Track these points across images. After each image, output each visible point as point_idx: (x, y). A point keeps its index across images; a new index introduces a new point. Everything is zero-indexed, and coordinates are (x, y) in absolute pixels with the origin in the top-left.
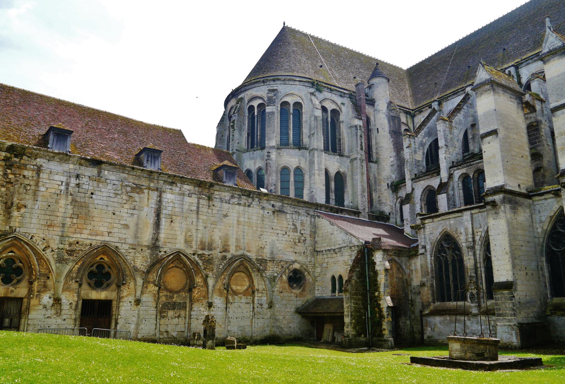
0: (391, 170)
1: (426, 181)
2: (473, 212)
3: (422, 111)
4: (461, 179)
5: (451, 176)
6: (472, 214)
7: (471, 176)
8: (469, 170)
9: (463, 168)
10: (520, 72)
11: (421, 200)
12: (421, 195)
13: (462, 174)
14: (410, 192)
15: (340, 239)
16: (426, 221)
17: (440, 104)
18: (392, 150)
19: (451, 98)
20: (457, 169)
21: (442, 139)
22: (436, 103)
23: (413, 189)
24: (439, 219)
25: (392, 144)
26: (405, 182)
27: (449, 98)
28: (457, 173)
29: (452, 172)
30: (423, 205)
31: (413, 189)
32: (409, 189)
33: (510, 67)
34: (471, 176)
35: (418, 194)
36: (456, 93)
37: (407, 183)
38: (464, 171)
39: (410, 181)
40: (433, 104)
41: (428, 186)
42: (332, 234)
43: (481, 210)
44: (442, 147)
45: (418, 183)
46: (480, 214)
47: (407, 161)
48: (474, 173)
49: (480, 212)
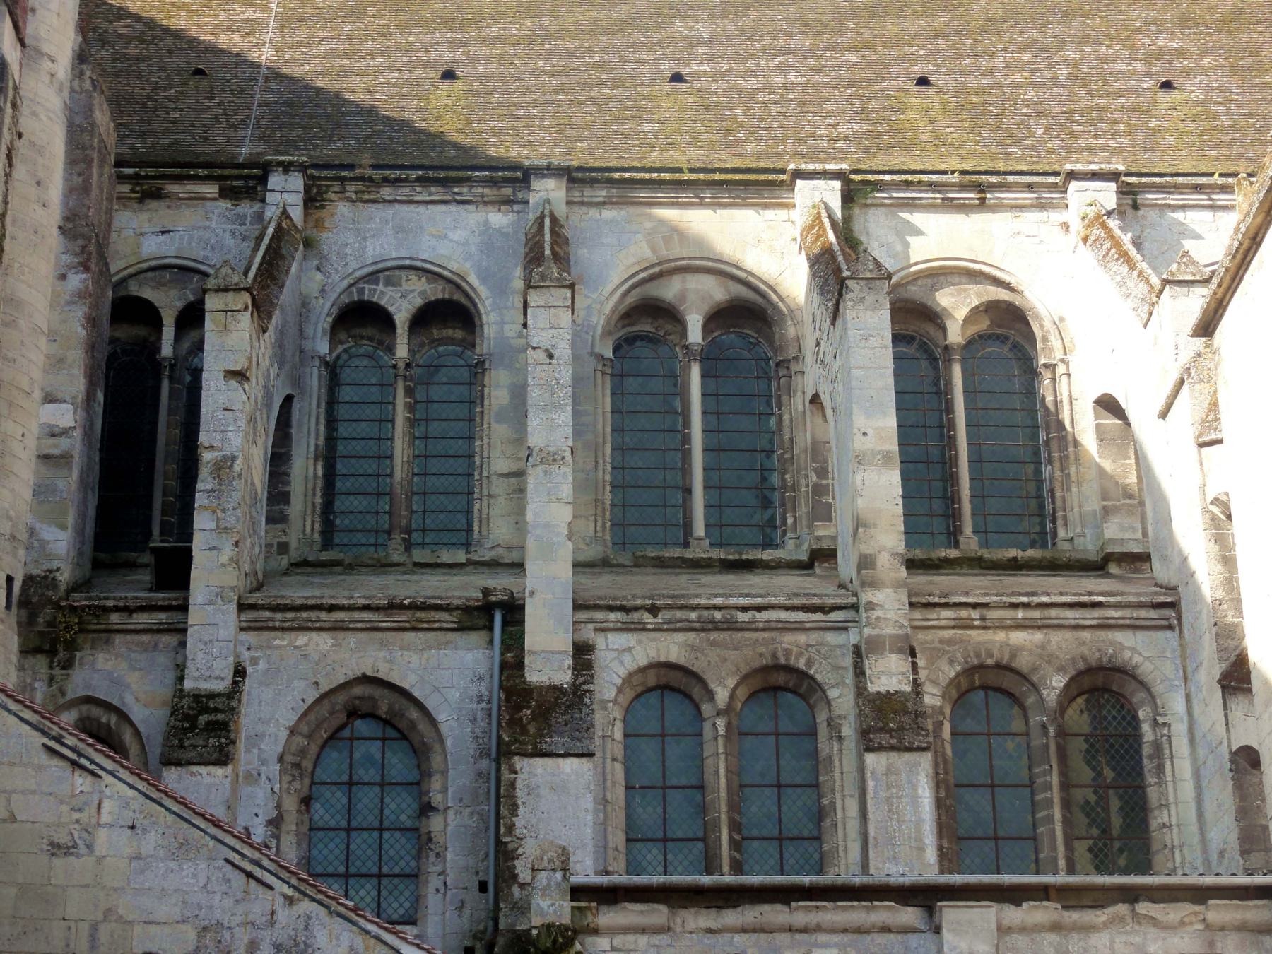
0: (41, 492)
1: (352, 639)
2: (1013, 915)
3: (157, 195)
4: (629, 694)
5: (582, 653)
6: (1003, 930)
7: (722, 695)
8: (713, 655)
9: (672, 627)
10: (857, 227)
11: (281, 759)
12: (292, 731)
13: (651, 666)
14: (221, 686)
15: (167, 910)
16: (608, 917)
17: (313, 200)
18: (77, 357)
19: (403, 192)
20: (625, 628)
21: (558, 407)
22: (296, 181)
23: (240, 672)
24: (731, 917)
25: (80, 312)
26: (184, 608)
27: (386, 192)
28: (622, 656)
29: (588, 633)
30: (290, 804)
31: (240, 672)
32: (207, 669)
33: (825, 175)
34: (722, 695)
35: (271, 717)
36: (444, 182)
37: (194, 616)
38: (673, 648)
39: (228, 616)
40: (275, 180)
41: (365, 679)
42: (57, 849)
43: (1074, 916)
44: (553, 459)
45: (281, 640)
46: (1052, 937)
47: (224, 466)
48: (745, 678)
49: (1056, 927)
